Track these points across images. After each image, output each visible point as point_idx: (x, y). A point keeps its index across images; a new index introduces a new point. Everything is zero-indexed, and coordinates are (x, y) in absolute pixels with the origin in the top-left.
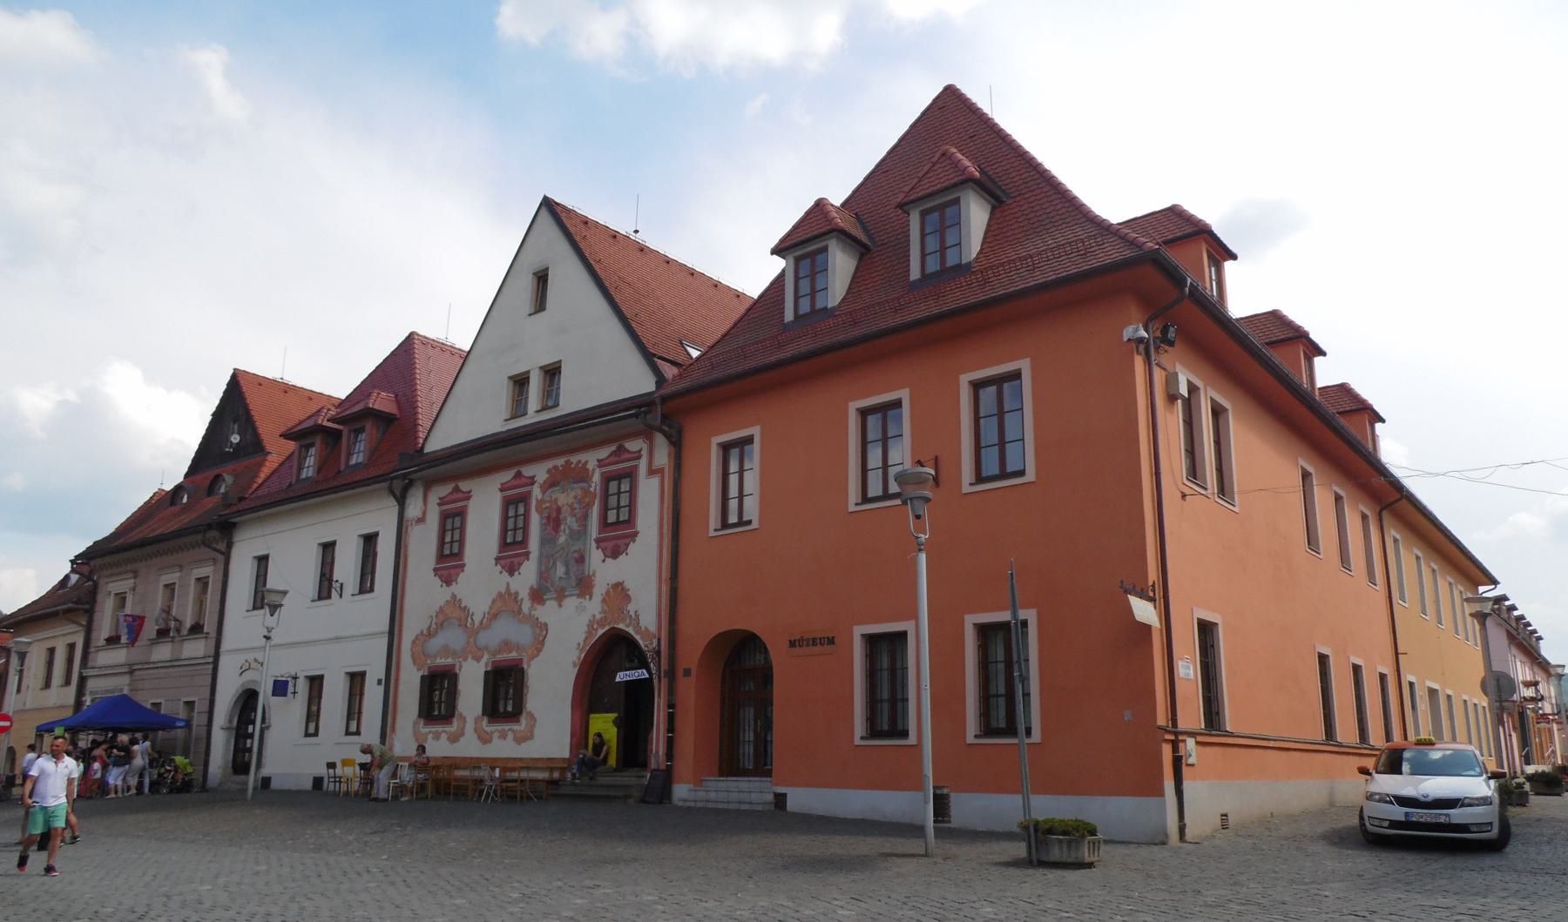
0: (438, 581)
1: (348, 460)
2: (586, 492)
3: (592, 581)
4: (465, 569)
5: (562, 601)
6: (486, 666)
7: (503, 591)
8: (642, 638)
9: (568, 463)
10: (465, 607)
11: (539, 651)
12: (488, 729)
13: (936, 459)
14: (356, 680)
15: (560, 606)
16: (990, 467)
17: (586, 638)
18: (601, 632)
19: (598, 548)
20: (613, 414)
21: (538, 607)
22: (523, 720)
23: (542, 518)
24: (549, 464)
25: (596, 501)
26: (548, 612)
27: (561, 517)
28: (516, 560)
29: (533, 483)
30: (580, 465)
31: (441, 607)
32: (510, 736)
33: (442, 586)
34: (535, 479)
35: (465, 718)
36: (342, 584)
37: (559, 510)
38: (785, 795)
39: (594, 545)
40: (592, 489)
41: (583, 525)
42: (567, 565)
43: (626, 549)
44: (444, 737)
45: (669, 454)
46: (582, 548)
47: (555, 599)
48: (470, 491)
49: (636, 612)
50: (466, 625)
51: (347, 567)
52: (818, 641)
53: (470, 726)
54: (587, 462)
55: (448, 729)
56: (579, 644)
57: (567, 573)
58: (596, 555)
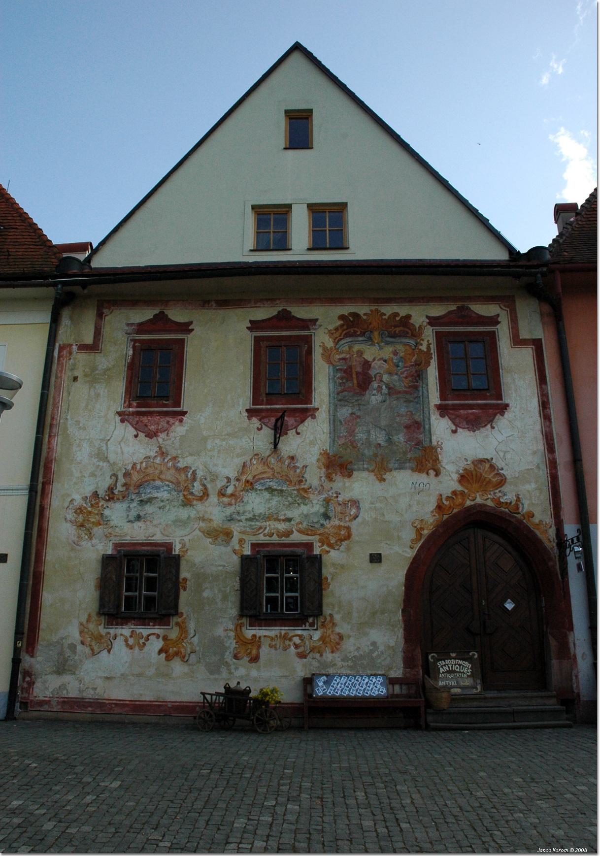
10: (186, 469)
27: (372, 372)
30: (398, 319)
37: (367, 365)
40: (424, 348)
48: (191, 323)
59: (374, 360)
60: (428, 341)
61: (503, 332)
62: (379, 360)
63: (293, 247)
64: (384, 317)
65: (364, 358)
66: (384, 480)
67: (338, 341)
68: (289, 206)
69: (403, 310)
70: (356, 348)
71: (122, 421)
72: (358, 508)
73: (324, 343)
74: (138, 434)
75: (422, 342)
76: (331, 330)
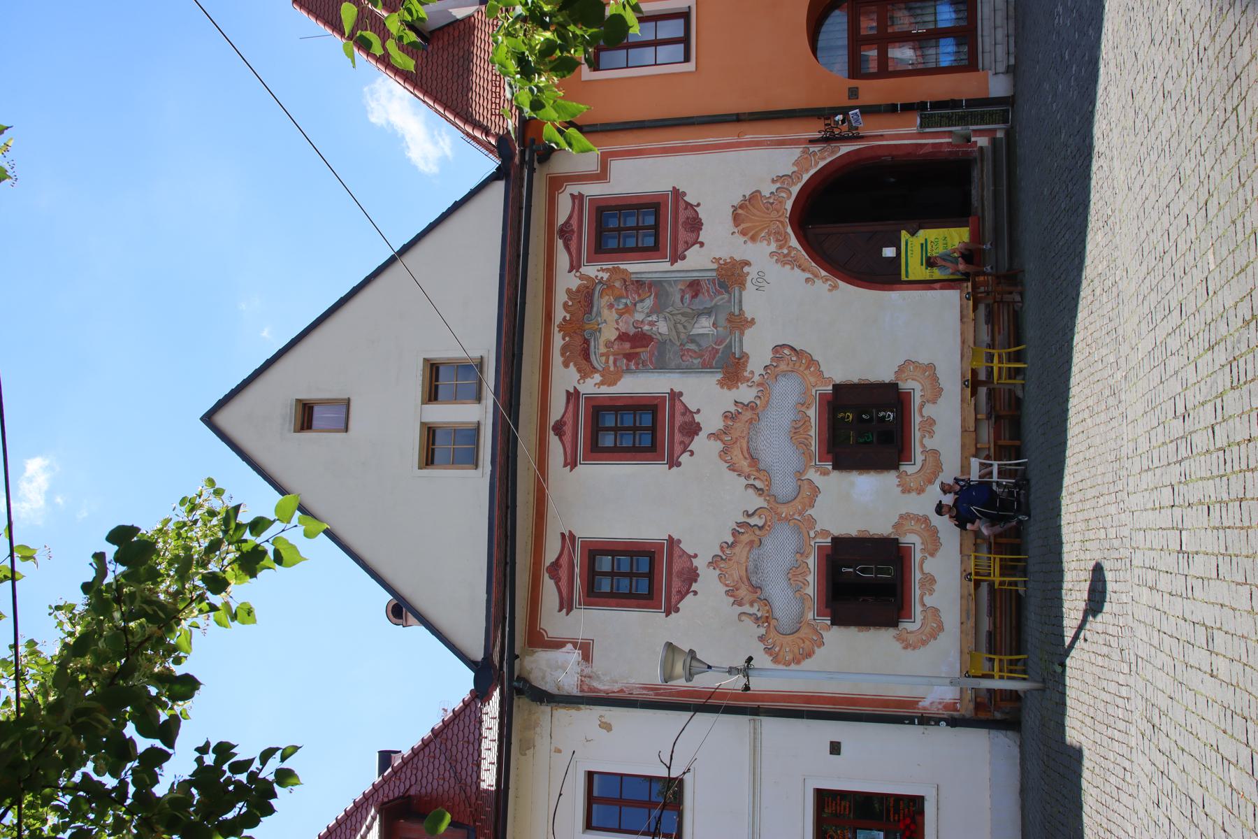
0: (687, 603)
2: (608, 286)
3: (726, 264)
4: (675, 537)
6: (825, 473)
7: (719, 445)
8: (807, 171)
9: (561, 328)
10: (735, 533)
11: (811, 362)
12: (919, 457)
15: (753, 322)
17: (799, 267)
18: (794, 242)
19: (684, 258)
21: (749, 368)
22: (905, 385)
23: (628, 370)
24: (557, 359)
25: (622, 267)
27: (632, 331)
28: (679, 420)
30: (570, 303)
32: (929, 410)
33: (695, 593)
34: (572, 390)
35: (901, 517)
37: (623, 337)
39: (679, 265)
40: (606, 276)
41: (650, 288)
44: (931, 566)
46: (679, 287)
47: (742, 334)
49: (773, 181)
50: (761, 528)
54: (569, 291)
55: (918, 556)
56: (807, 280)
57: (708, 312)
58: (697, 261)
59: (617, 329)
60: (598, 271)
61: (593, 190)
62: (617, 323)
63: (475, 420)
64: (568, 318)
65: (615, 340)
66: (753, 319)
67: (594, 368)
68: (423, 424)
69: (561, 297)
70: (603, 350)
71: (677, 610)
72: (784, 346)
73: (596, 384)
74: (693, 591)
75: (599, 278)
76: (581, 376)
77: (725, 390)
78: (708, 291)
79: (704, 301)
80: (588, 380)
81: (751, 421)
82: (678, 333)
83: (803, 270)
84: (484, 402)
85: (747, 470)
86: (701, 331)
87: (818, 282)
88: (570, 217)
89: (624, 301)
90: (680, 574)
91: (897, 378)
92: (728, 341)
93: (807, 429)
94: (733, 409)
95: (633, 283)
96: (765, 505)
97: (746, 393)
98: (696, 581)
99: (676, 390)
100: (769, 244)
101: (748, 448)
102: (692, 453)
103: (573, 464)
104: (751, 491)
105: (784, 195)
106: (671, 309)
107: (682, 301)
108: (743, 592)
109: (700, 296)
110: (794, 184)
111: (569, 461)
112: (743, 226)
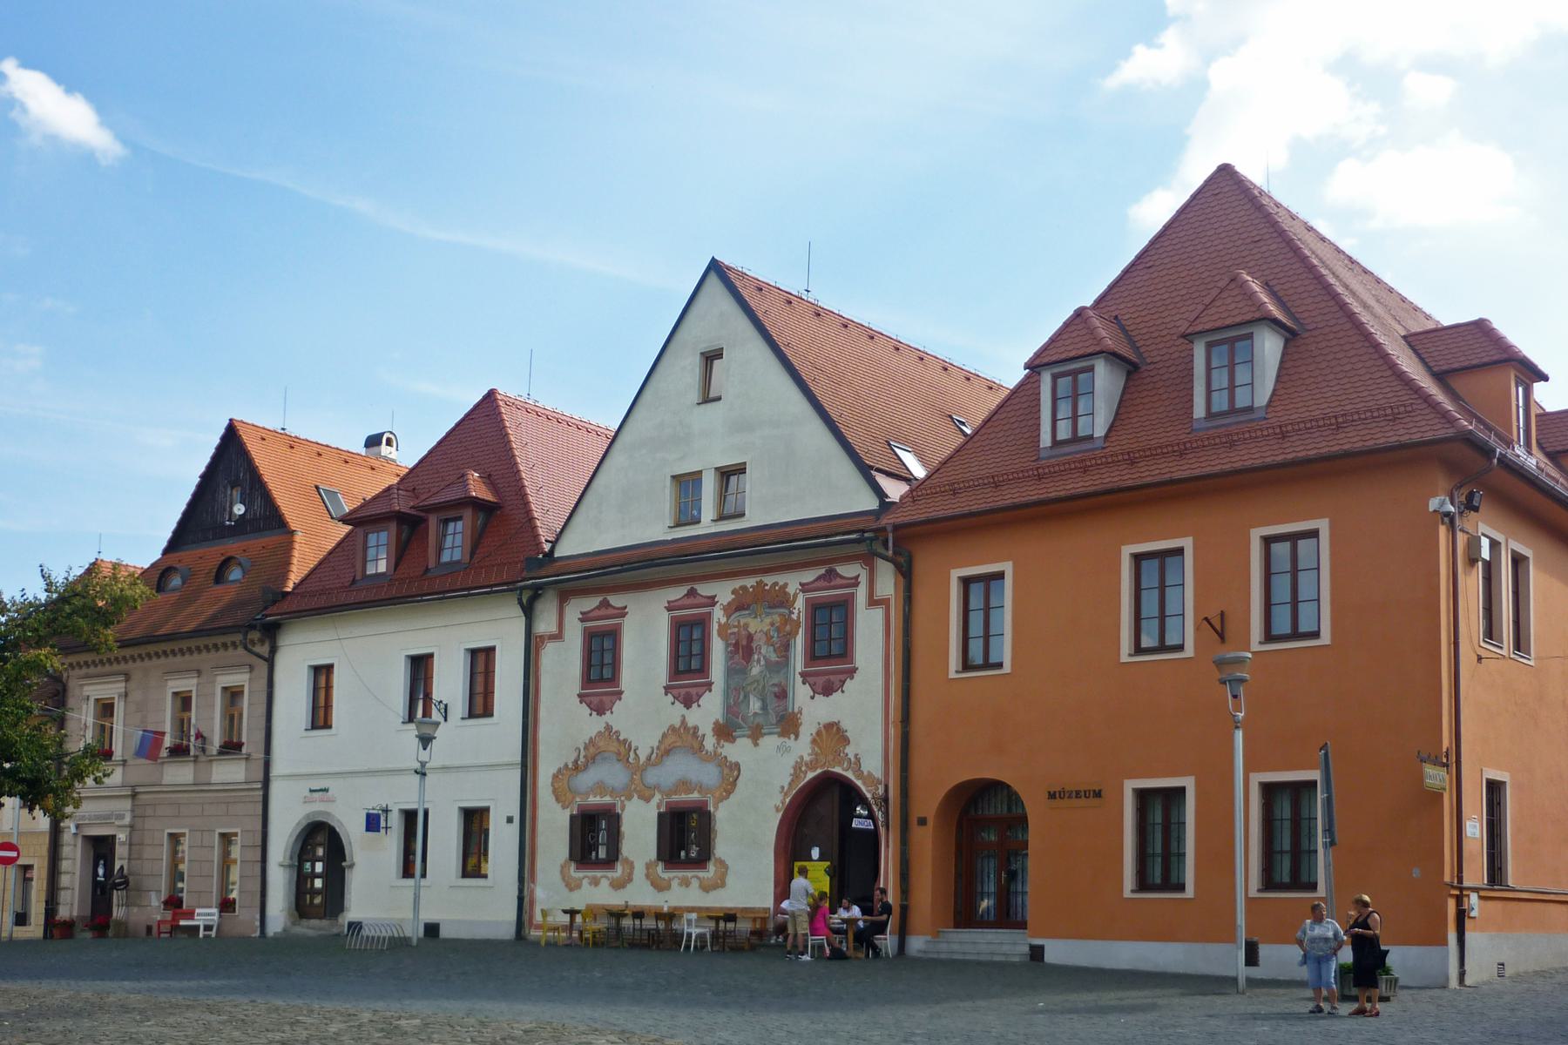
0: (585, 710)
1: (439, 555)
2: (787, 620)
4: (623, 696)
5: (758, 739)
6: (659, 806)
8: (864, 783)
9: (759, 583)
10: (625, 741)
11: (729, 793)
12: (666, 875)
13: (1222, 614)
14: (474, 821)
15: (756, 745)
16: (1282, 624)
17: (792, 781)
18: (810, 775)
19: (804, 683)
20: (827, 536)
21: (726, 744)
22: (711, 867)
23: (727, 645)
24: (737, 583)
26: (739, 750)
27: (754, 645)
28: (693, 691)
29: (714, 604)
31: (591, 738)
32: (695, 883)
33: (591, 715)
34: (716, 600)
35: (632, 863)
36: (446, 706)
37: (750, 638)
38: (1042, 948)
39: (799, 679)
40: (794, 617)
42: (764, 701)
43: (842, 686)
44: (605, 883)
45: (896, 584)
47: (748, 737)
48: (626, 607)
49: (856, 755)
51: (450, 684)
52: (1083, 793)
53: (639, 871)
54: (786, 585)
55: (610, 874)
56: (783, 787)
57: (764, 708)
58: (801, 693)
64: (766, 588)
67: (730, 616)
69: (781, 579)
77: (712, 726)
78: (779, 706)
79: (773, 703)
80: (722, 612)
81: (692, 748)
82: (752, 683)
83: (790, 784)
84: (713, 524)
85: (662, 747)
86: (751, 703)
87: (780, 797)
88: (842, 577)
89: (776, 635)
90: (601, 702)
91: (716, 859)
92: (744, 725)
93: (686, 793)
94: (700, 733)
95: (788, 641)
96: (641, 763)
97: (710, 743)
98: (598, 714)
99: (713, 687)
100: (809, 755)
101: (674, 747)
102: (673, 704)
103: (669, 609)
104: (649, 751)
105: (846, 764)
106: (768, 676)
107: (773, 685)
108: (592, 750)
109: (775, 700)
110: (854, 773)
111: (672, 604)
112: (824, 732)
